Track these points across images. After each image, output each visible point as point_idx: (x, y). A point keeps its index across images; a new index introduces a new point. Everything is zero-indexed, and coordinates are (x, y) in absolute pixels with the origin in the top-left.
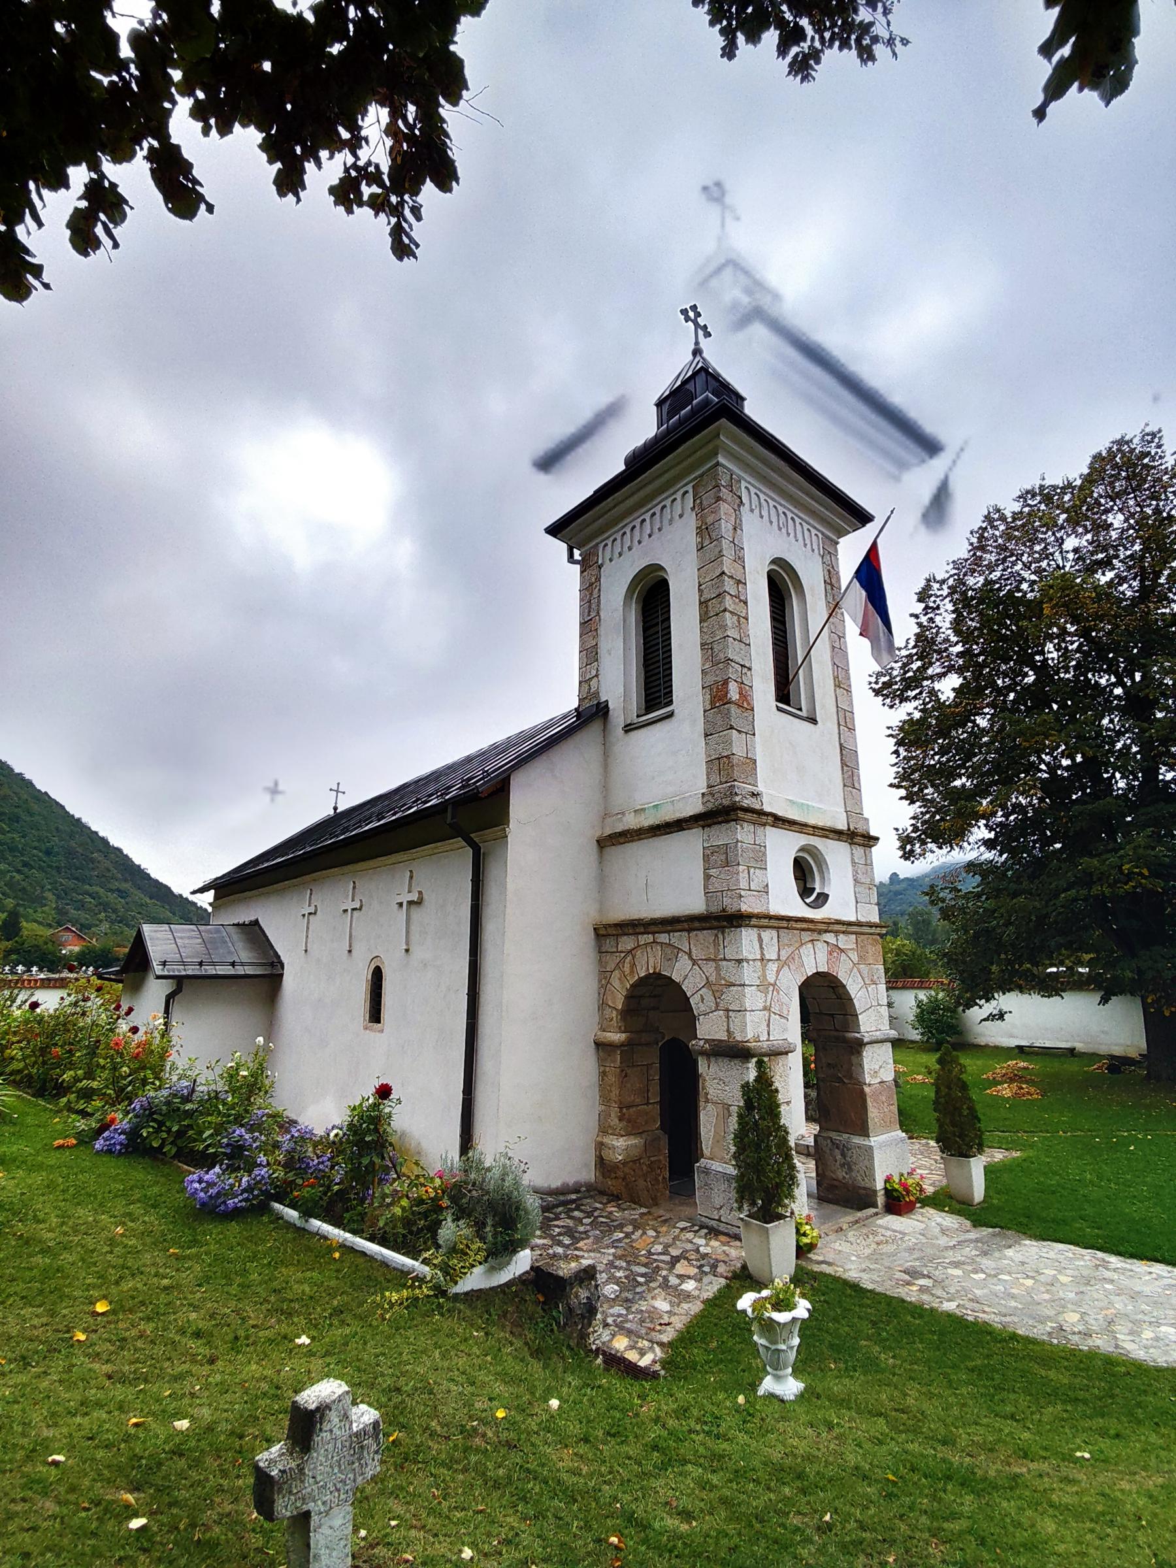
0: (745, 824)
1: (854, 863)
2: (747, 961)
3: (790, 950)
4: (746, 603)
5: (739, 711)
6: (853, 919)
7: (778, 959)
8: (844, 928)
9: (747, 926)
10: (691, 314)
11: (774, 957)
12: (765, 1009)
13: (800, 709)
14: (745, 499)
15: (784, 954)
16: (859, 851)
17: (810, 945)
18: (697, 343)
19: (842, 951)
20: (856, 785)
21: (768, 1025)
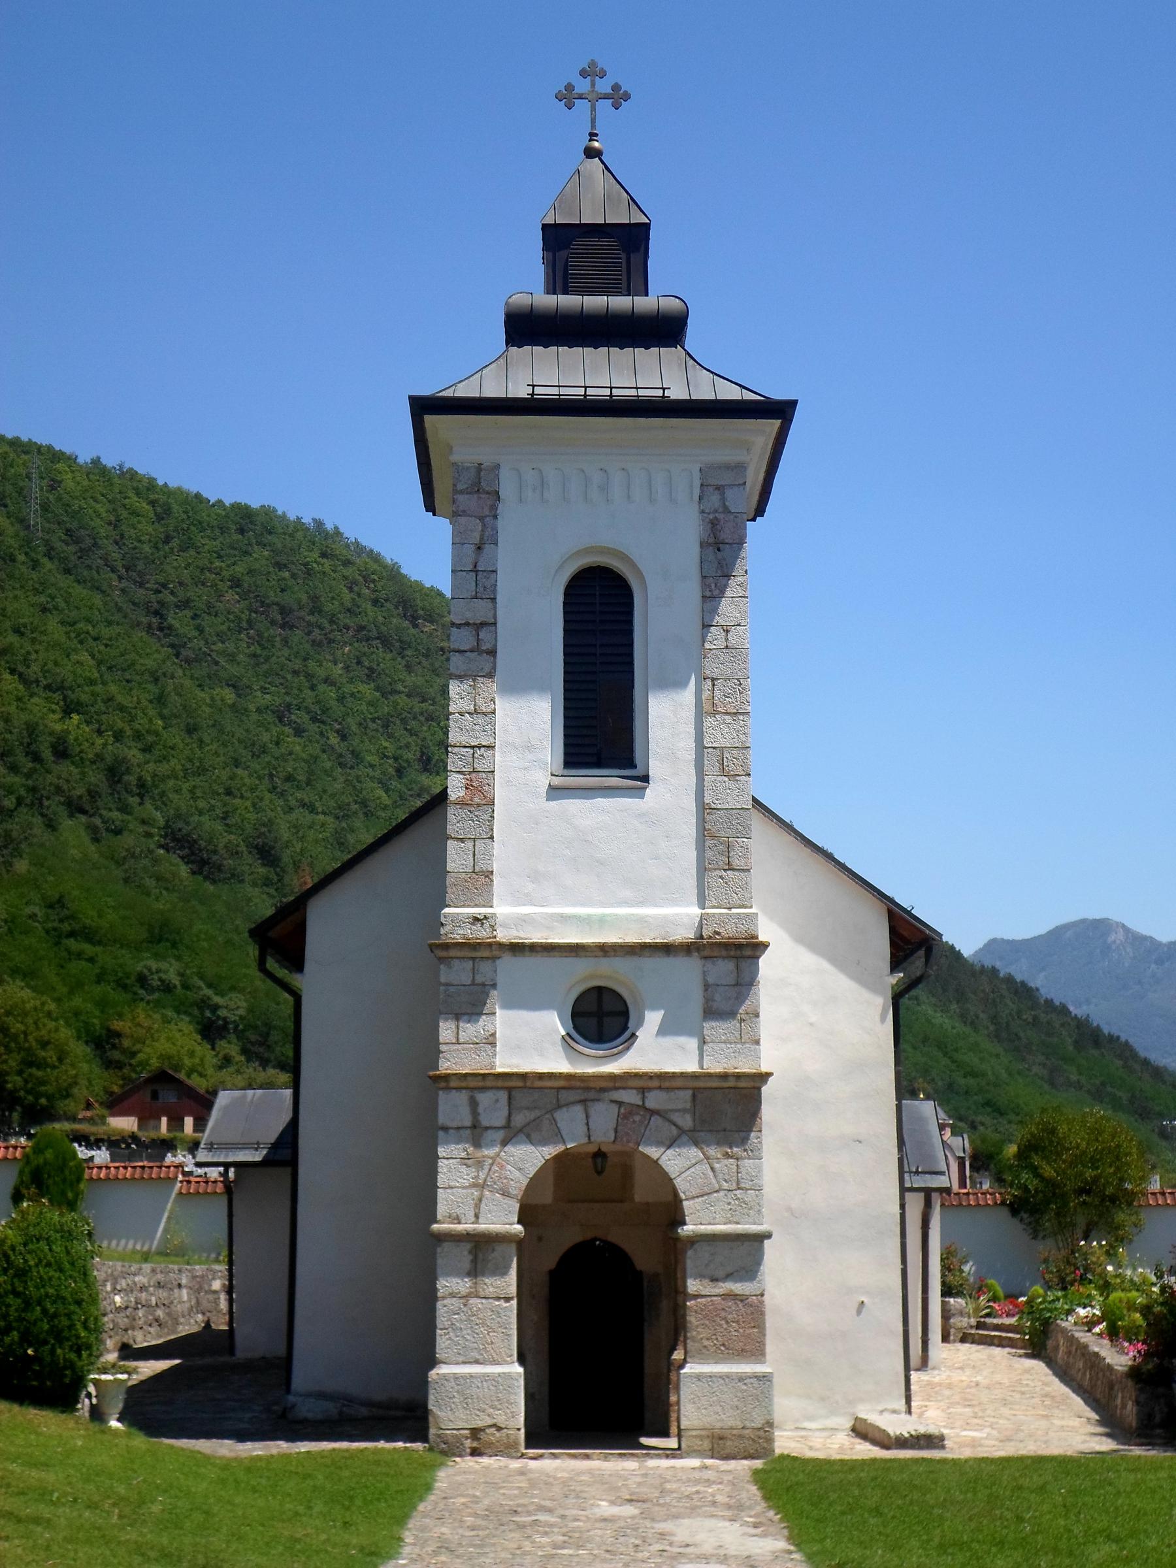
0: (456, 963)
1: (706, 986)
2: (445, 1129)
3: (531, 1115)
4: (493, 652)
5: (462, 813)
6: (692, 1067)
7: (507, 1126)
8: (655, 1083)
9: (448, 1089)
10: (583, 85)
11: (501, 1122)
12: (474, 1185)
13: (635, 767)
14: (507, 489)
15: (519, 1120)
16: (723, 969)
17: (578, 1110)
18: (593, 136)
19: (653, 1112)
20: (736, 863)
21: (477, 1206)
